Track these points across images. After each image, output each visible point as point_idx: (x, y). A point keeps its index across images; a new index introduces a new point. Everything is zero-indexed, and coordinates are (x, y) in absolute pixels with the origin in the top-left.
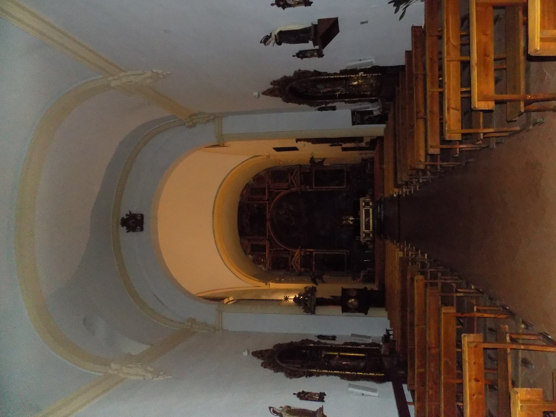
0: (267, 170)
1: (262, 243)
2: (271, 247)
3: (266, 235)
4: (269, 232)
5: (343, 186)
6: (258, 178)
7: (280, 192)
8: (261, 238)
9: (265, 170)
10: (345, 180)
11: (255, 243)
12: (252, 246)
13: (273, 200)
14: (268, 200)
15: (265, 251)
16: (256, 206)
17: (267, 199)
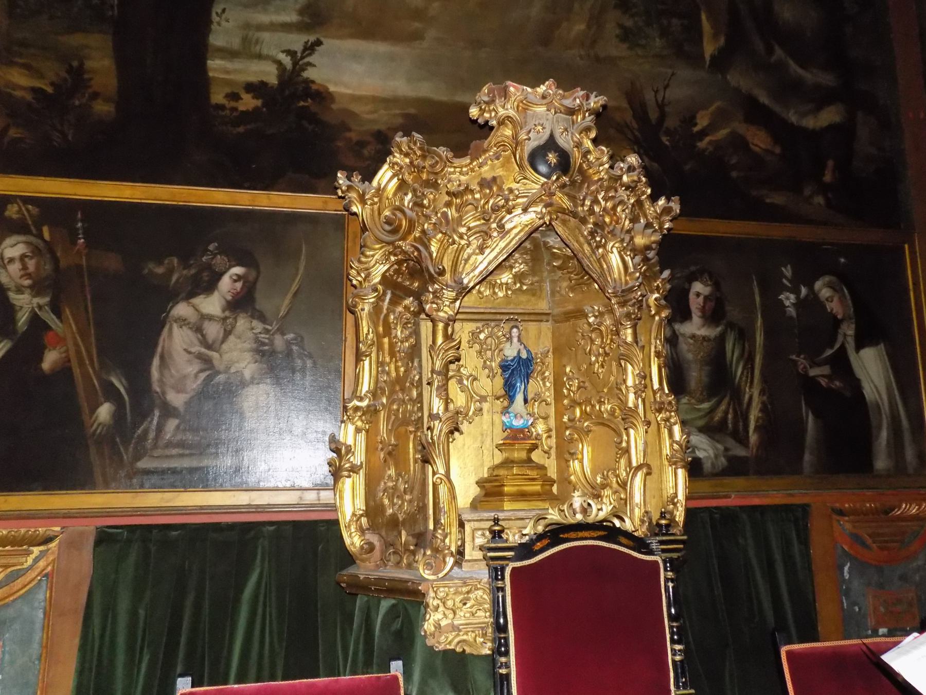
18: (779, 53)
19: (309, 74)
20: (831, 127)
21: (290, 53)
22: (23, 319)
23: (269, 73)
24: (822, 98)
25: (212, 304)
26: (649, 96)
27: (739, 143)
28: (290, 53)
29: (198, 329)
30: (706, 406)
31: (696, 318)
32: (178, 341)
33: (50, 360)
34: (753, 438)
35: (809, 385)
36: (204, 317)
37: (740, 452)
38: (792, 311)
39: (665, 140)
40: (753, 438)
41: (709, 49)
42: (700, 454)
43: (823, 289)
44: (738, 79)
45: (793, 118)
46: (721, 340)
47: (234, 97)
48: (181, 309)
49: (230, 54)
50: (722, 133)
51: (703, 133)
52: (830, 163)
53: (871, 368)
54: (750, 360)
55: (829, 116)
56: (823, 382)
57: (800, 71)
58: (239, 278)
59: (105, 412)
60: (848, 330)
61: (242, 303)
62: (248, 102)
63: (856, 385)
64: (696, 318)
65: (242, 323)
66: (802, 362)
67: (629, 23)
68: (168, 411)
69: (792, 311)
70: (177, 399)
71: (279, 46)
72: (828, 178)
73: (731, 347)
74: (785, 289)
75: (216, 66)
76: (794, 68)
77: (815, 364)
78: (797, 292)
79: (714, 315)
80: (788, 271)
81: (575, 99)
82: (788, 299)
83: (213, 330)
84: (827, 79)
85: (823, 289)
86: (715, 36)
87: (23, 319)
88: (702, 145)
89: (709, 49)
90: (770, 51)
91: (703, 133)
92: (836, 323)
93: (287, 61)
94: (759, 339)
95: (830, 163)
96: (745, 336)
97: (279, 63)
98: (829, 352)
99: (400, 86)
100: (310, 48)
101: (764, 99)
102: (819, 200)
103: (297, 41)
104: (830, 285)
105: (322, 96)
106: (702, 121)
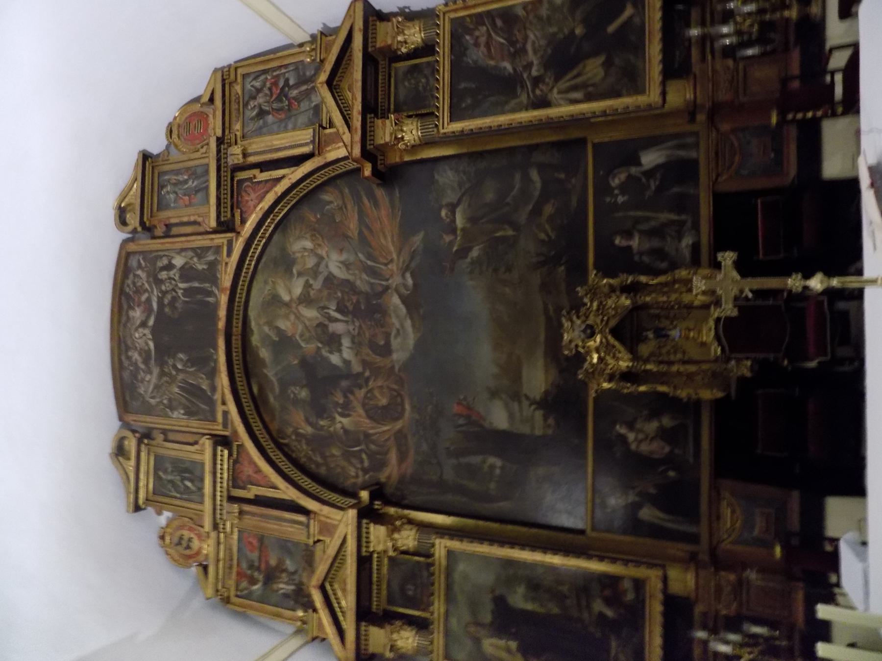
0: (226, 77)
1: (187, 453)
2: (235, 481)
3: (214, 420)
4: (224, 403)
5: (639, 90)
6: (187, 125)
7: (278, 180)
8: (195, 424)
9: (216, 71)
10: (654, 50)
11: (173, 450)
12: (160, 462)
13: (243, 221)
14: (226, 226)
15: (202, 502)
16: (178, 261)
17: (213, 223)
18: (509, 200)
19: (538, 398)
20: (539, 172)
21: (530, 405)
22: (637, 499)
23: (539, 414)
24: (526, 178)
25: (631, 436)
26: (534, 260)
27: (551, 219)
28: (530, 405)
29: (641, 441)
30: (669, 239)
31: (631, 243)
32: (645, 448)
33: (652, 491)
34: (683, 217)
35: (660, 189)
36: (636, 439)
37: (689, 224)
38: (626, 198)
39: (553, 253)
40: (683, 217)
41: (510, 232)
42: (690, 242)
43: (615, 182)
44: (522, 217)
45: (537, 193)
46: (641, 232)
47: (549, 426)
48: (633, 447)
49: (533, 428)
50: (547, 227)
51: (548, 235)
52: (556, 175)
53: (650, 159)
54: (648, 219)
55: (534, 175)
56: (657, 183)
57: (515, 190)
58: (621, 426)
59: (672, 474)
60: (634, 170)
61: (631, 426)
62: (551, 421)
63: (658, 167)
64: (631, 243)
65: (639, 425)
66: (648, 194)
67: (503, 270)
68: (671, 452)
69: (626, 198)
70: (667, 449)
71: (528, 410)
72: (562, 176)
73: (644, 227)
74: (616, 201)
75: (538, 432)
76: (515, 192)
77: (649, 186)
78: (617, 195)
79: (629, 235)
80: (608, 199)
81: (567, 324)
82: (621, 199)
83: (641, 436)
84: (518, 176)
85: (615, 182)
86: (504, 229)
87: (637, 499)
88: (553, 237)
89: (510, 232)
90: (508, 204)
91: (548, 235)
92: (630, 177)
93: (533, 407)
94: (639, 213)
95: (556, 175)
96: (637, 221)
97: (534, 410)
98: (644, 180)
99: (540, 363)
100: (527, 398)
101: (530, 207)
102: (573, 181)
103: (525, 403)
104: (613, 178)
105: (546, 393)
106: (543, 236)
